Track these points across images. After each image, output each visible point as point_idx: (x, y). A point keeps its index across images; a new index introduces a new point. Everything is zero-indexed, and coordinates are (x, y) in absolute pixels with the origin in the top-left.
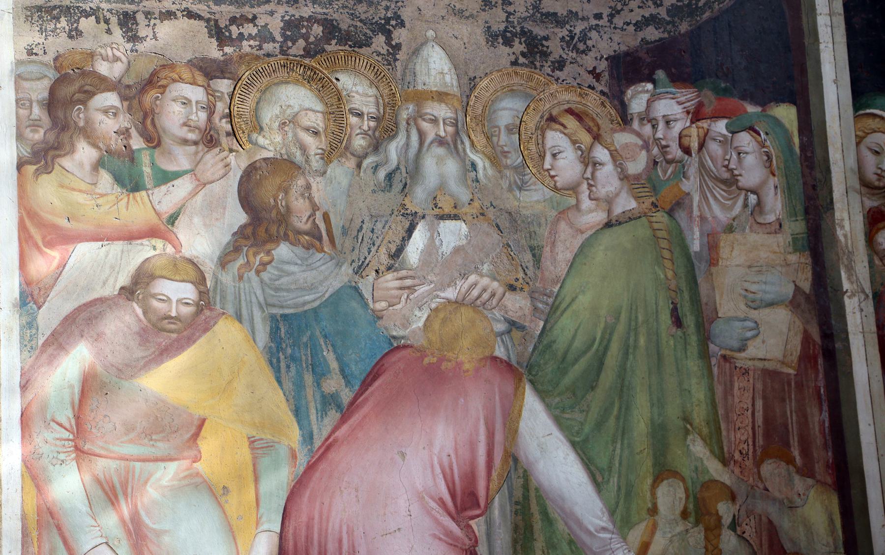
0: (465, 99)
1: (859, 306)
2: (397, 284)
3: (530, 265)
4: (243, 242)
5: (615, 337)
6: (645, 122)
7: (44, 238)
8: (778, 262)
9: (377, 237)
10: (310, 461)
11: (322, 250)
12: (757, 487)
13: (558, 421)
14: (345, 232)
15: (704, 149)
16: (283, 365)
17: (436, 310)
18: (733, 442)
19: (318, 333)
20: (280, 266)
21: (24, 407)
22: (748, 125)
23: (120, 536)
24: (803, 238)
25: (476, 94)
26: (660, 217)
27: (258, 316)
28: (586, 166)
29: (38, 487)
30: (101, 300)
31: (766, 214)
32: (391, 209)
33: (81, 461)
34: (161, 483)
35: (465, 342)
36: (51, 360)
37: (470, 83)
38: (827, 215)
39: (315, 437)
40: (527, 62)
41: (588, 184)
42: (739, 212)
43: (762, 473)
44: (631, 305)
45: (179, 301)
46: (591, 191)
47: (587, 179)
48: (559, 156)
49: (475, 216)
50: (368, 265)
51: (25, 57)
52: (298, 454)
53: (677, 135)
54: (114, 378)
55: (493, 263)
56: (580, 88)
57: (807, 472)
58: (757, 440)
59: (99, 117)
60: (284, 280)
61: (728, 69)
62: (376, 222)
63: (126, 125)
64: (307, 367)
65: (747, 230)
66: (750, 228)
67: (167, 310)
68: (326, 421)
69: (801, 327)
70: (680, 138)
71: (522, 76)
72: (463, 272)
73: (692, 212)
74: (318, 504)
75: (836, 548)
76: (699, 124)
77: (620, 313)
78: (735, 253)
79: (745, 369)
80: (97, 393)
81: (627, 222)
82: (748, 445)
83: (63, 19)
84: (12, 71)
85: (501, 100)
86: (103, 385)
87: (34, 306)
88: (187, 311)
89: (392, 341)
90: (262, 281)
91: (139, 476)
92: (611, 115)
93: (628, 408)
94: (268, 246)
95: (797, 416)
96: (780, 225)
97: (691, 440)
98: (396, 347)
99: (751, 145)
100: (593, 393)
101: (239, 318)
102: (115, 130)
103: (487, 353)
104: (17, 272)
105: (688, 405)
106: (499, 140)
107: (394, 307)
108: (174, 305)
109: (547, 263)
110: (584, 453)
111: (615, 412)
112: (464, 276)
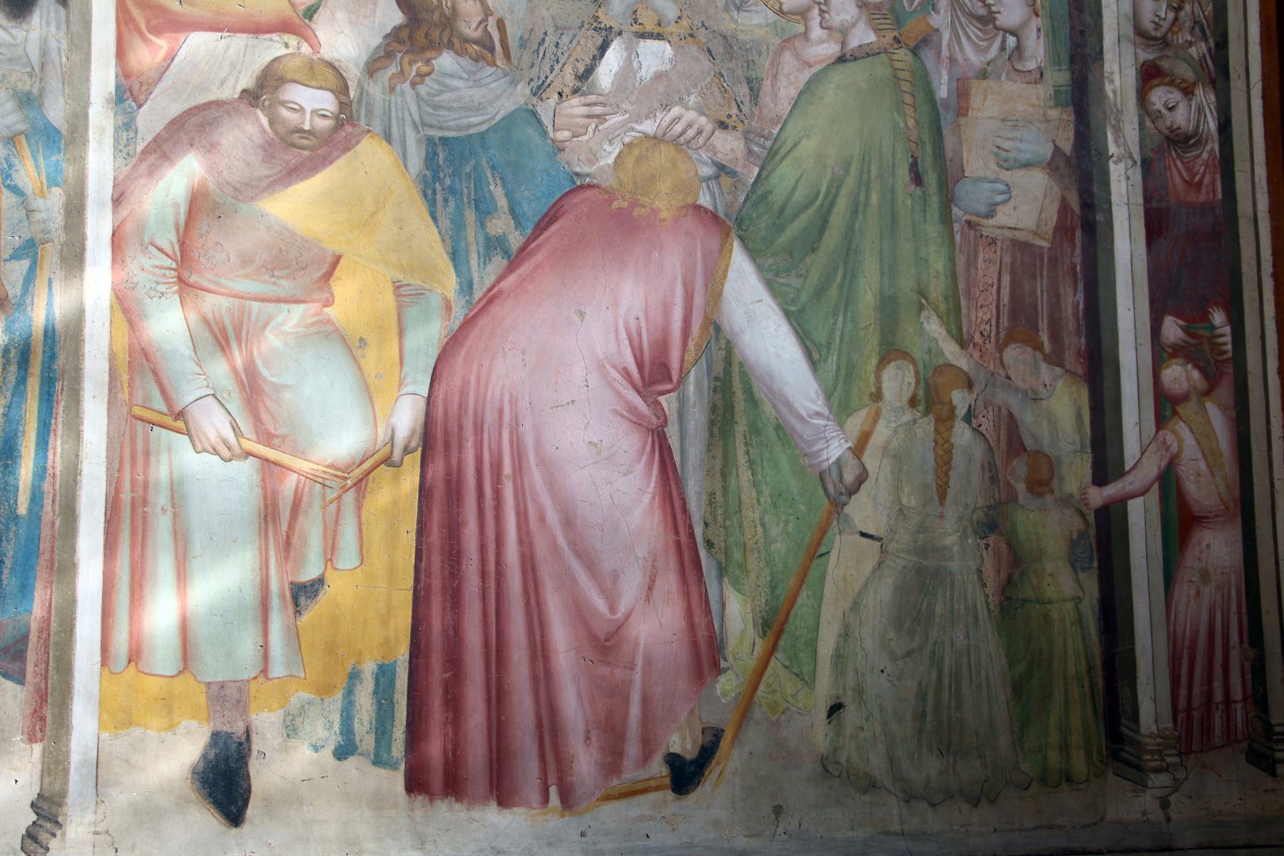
1: (1126, 173)
2: (584, 110)
3: (747, 100)
4: (396, 46)
5: (844, 192)
7: (148, 22)
8: (1035, 117)
9: (563, 54)
10: (467, 315)
11: (494, 64)
12: (998, 374)
13: (771, 286)
14: (523, 44)
16: (439, 197)
17: (629, 146)
18: (974, 322)
19: (484, 163)
20: (442, 79)
21: (116, 225)
23: (230, 388)
24: (1067, 91)
26: (903, 55)
27: (411, 136)
29: (131, 323)
30: (217, 104)
31: (1026, 61)
32: (580, 22)
33: (185, 295)
34: (283, 328)
35: (664, 186)
36: (152, 172)
39: (476, 286)
41: (820, 9)
42: (995, 56)
43: (1004, 358)
45: (314, 112)
46: (823, 18)
49: (683, 37)
50: (549, 85)
52: (453, 305)
54: (230, 199)
55: (701, 94)
57: (1055, 359)
58: (1001, 321)
60: (446, 96)
62: (562, 34)
64: (469, 202)
65: (1003, 77)
66: (1007, 75)
67: (299, 121)
68: (490, 268)
69: (1059, 194)
72: (664, 102)
73: (940, 52)
74: (475, 365)
75: (1083, 447)
77: (850, 164)
78: (988, 103)
79: (992, 238)
80: (208, 216)
81: (863, 58)
82: (991, 326)
86: (216, 206)
87: (133, 104)
88: (323, 124)
89: (575, 178)
90: (418, 96)
93: (854, 276)
94: (428, 54)
96: (1042, 74)
97: (925, 316)
98: (579, 186)
100: (813, 255)
101: (388, 138)
103: (689, 201)
104: (113, 61)
105: (925, 277)
107: (580, 139)
108: (308, 116)
109: (766, 98)
110: (799, 325)
111: (839, 279)
112: (666, 107)
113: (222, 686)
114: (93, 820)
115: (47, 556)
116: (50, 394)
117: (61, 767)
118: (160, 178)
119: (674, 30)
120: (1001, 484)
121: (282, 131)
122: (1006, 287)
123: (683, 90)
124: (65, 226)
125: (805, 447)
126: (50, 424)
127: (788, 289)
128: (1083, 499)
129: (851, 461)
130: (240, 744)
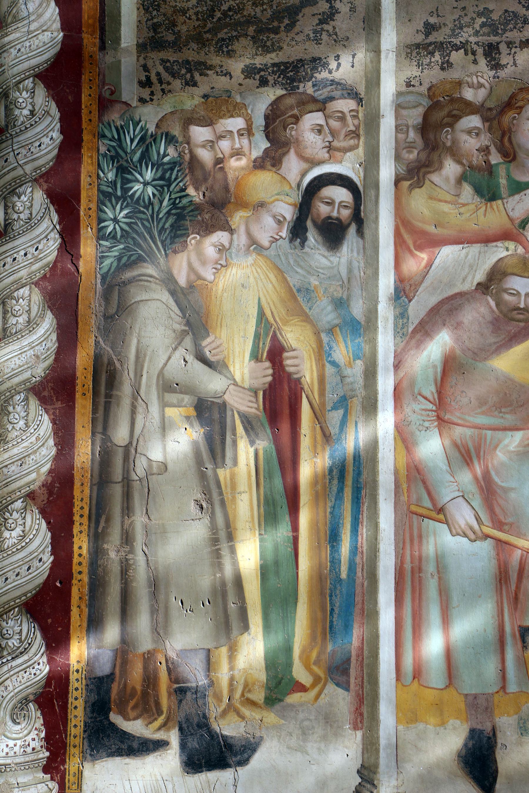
23: (473, 491)
30: (461, 295)
33: (442, 428)
34: (508, 448)
36: (419, 345)
51: (404, 89)
54: (470, 360)
59: (464, 137)
63: (487, 143)
67: (517, 302)
80: (456, 373)
83: (437, 54)
84: (393, 102)
87: (406, 299)
91: (490, 443)
102: (477, 148)
108: (523, 298)
113: (476, 696)
114: (396, 784)
115: (360, 606)
116: (358, 498)
117: (374, 747)
118: (424, 349)
121: (505, 309)
124: (365, 385)
126: (359, 518)
130: (489, 738)
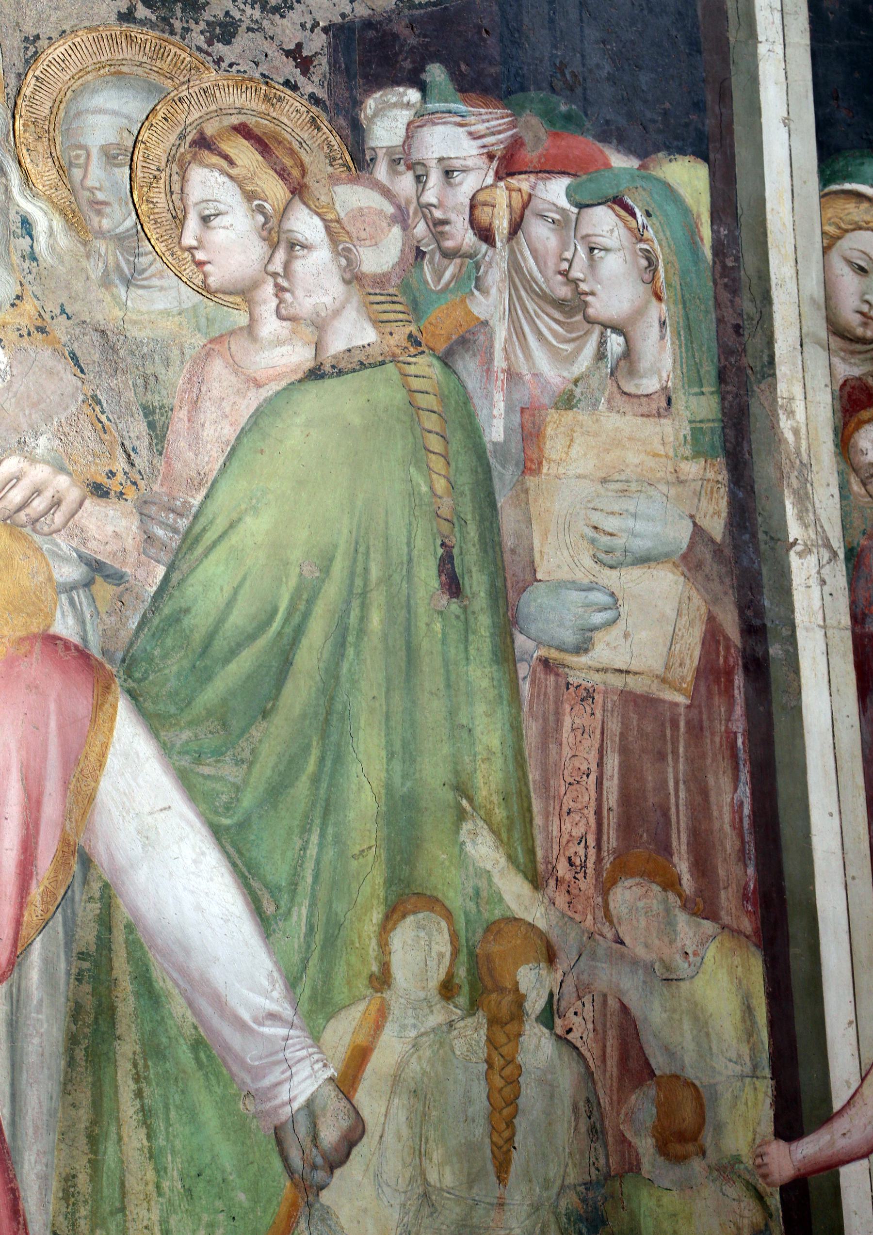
0: (13, 81)
1: (819, 573)
3: (143, 446)
5: (320, 609)
6: (402, 168)
12: (601, 935)
15: (520, 233)
22: (611, 193)
25: (37, 73)
28: (274, 247)
31: (641, 377)
37: (26, 48)
38: (762, 386)
40: (154, 18)
41: (276, 285)
42: (588, 368)
43: (612, 906)
44: (357, 543)
47: (275, 275)
48: (215, 222)
49: (24, 332)
53: (467, 202)
55: (61, 435)
56: (267, 83)
58: (605, 838)
61: (574, 75)
65: (602, 406)
66: (609, 402)
69: (703, 610)
70: (472, 207)
71: (142, 46)
73: (491, 360)
75: (755, 1067)
76: (514, 181)
77: (331, 560)
78: (576, 450)
79: (585, 689)
82: (586, 847)
85: (95, 91)
92: (329, 145)
93: (339, 759)
95: (688, 790)
96: (669, 402)
97: (469, 832)
99: (616, 234)
100: (265, 724)
105: (467, 759)
106: (85, 176)
110: (239, 852)
111: (311, 766)
119: (8, 319)
120: (610, 1139)
122: (612, 777)
123: (25, 427)
125: (248, 1080)
127: (218, 786)
128: (759, 1166)
129: (333, 1102)
